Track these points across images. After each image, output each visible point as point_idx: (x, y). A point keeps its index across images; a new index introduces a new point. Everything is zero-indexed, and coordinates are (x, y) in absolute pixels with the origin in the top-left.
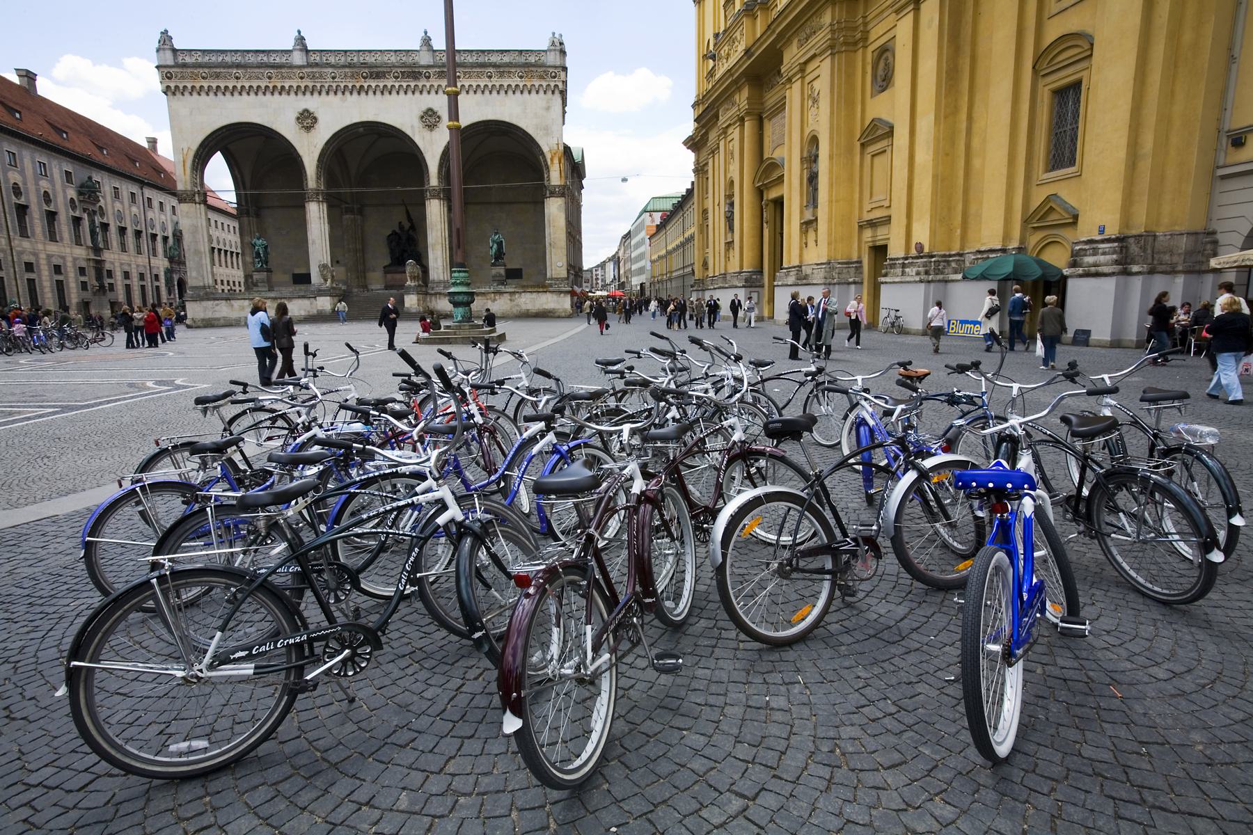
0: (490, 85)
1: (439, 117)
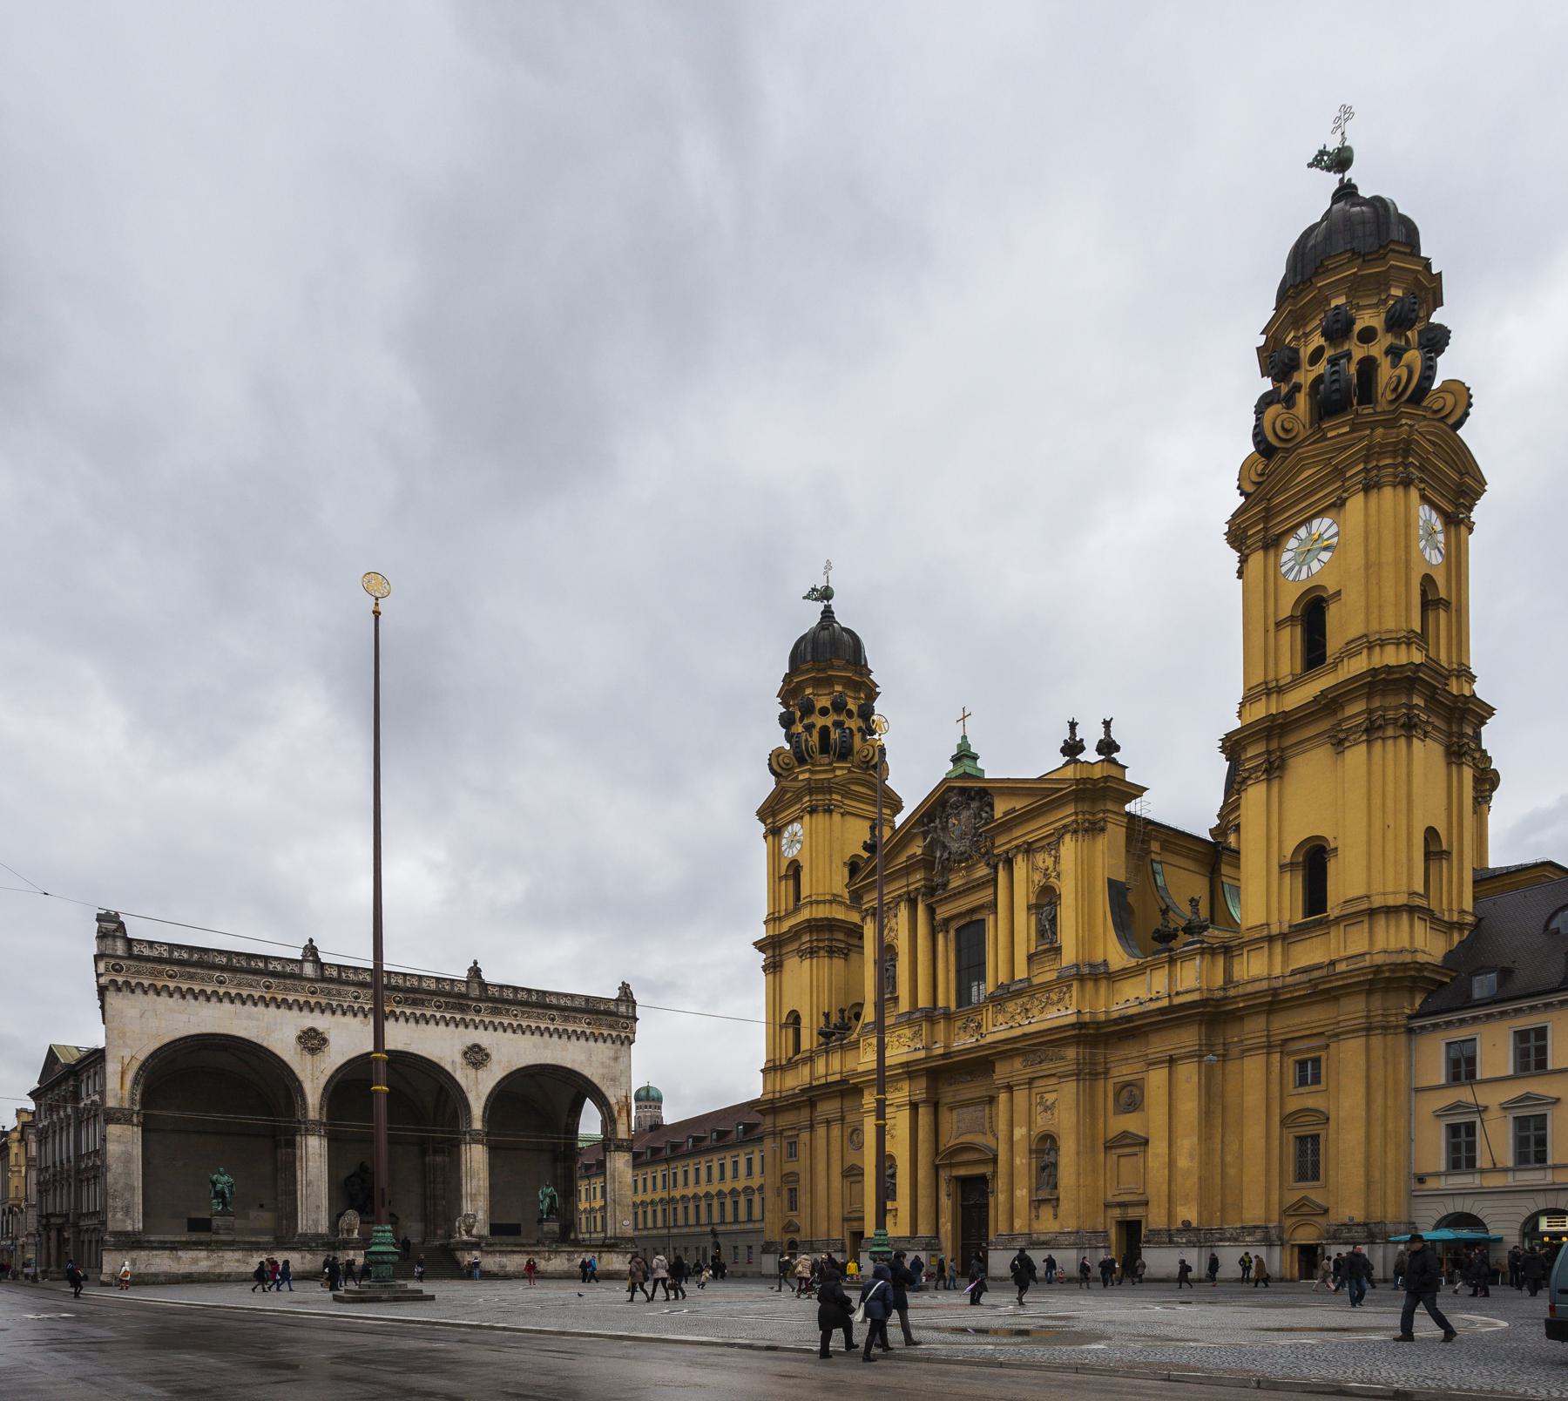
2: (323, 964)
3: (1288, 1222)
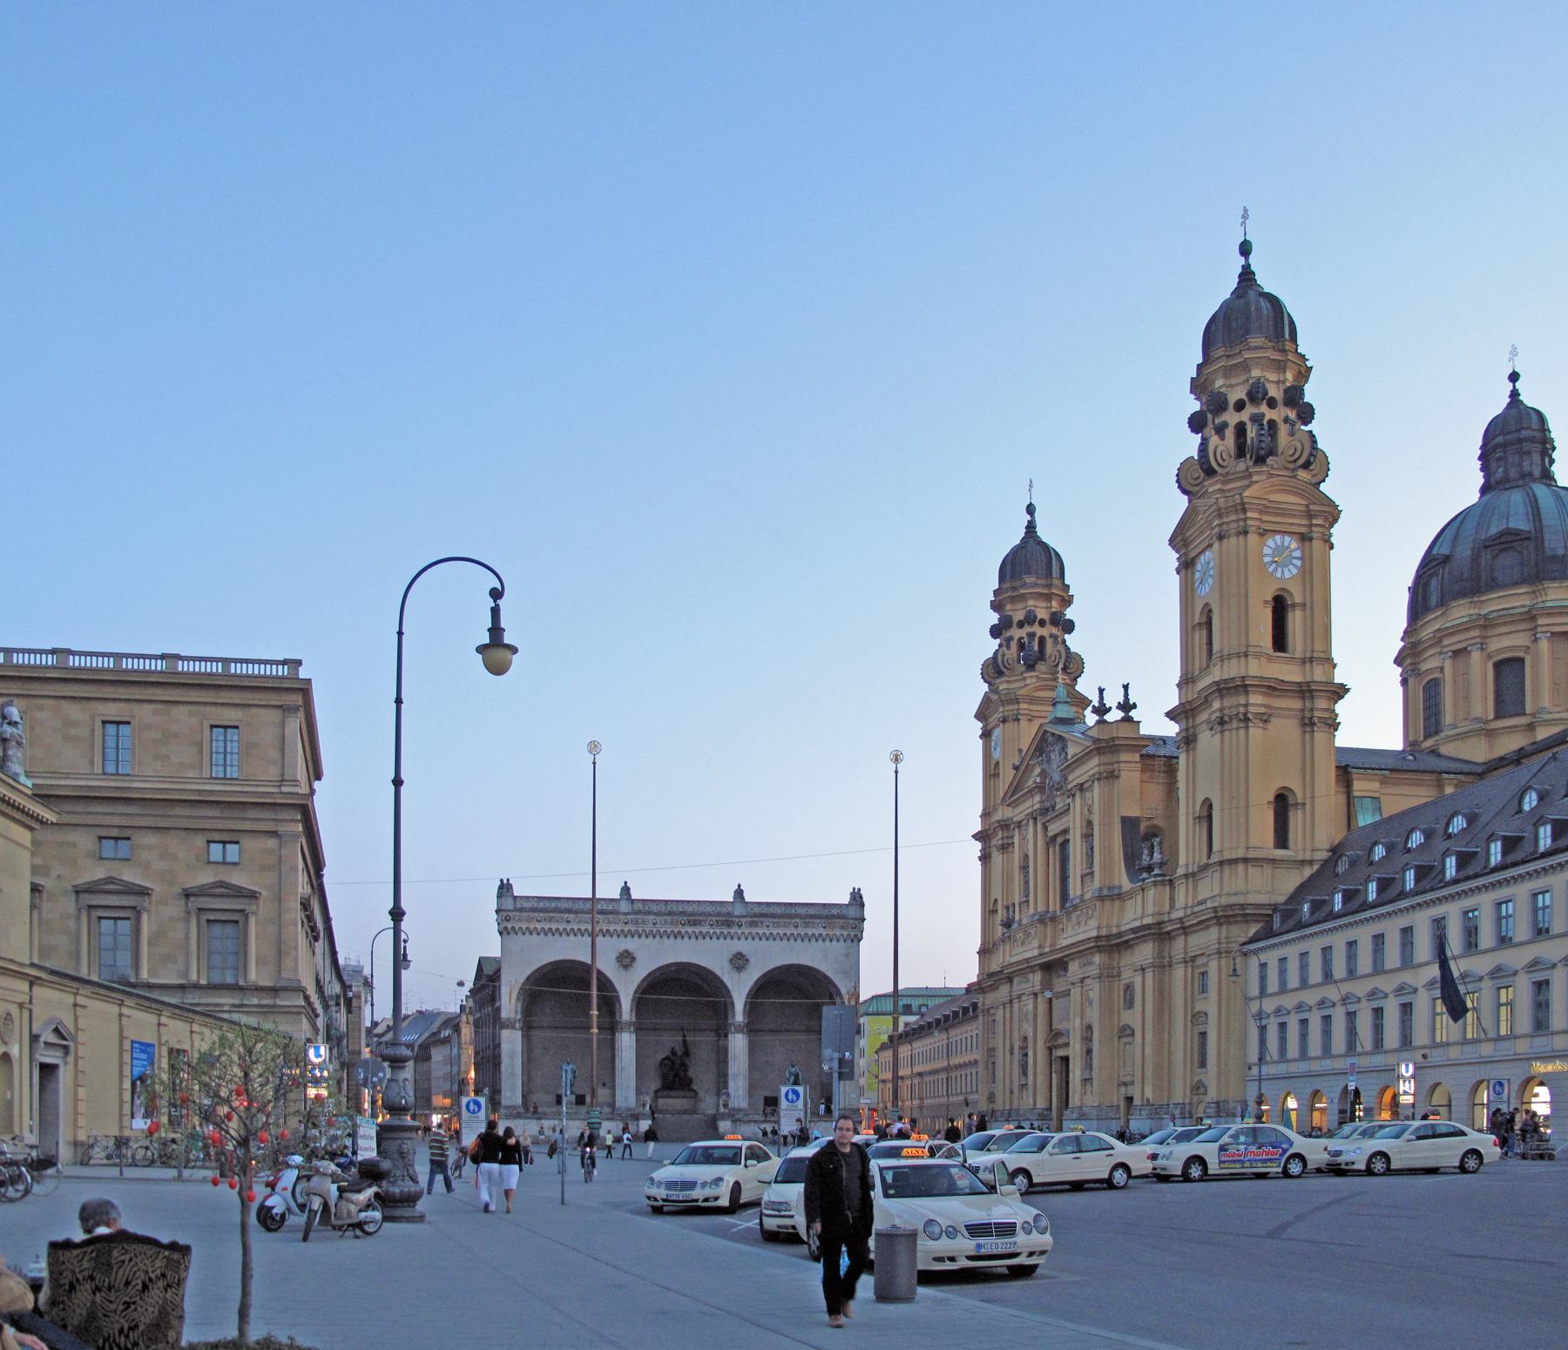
0: (796, 933)
1: (747, 960)
2: (633, 901)
3: (1195, 1099)
